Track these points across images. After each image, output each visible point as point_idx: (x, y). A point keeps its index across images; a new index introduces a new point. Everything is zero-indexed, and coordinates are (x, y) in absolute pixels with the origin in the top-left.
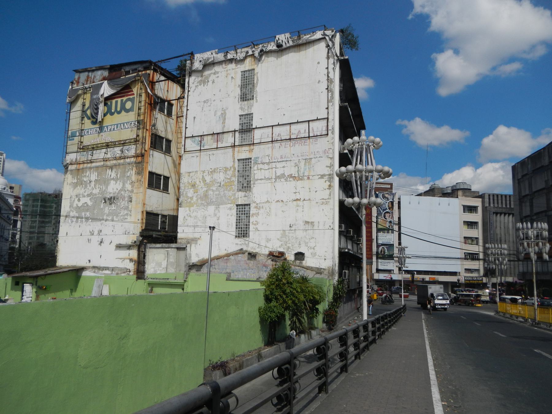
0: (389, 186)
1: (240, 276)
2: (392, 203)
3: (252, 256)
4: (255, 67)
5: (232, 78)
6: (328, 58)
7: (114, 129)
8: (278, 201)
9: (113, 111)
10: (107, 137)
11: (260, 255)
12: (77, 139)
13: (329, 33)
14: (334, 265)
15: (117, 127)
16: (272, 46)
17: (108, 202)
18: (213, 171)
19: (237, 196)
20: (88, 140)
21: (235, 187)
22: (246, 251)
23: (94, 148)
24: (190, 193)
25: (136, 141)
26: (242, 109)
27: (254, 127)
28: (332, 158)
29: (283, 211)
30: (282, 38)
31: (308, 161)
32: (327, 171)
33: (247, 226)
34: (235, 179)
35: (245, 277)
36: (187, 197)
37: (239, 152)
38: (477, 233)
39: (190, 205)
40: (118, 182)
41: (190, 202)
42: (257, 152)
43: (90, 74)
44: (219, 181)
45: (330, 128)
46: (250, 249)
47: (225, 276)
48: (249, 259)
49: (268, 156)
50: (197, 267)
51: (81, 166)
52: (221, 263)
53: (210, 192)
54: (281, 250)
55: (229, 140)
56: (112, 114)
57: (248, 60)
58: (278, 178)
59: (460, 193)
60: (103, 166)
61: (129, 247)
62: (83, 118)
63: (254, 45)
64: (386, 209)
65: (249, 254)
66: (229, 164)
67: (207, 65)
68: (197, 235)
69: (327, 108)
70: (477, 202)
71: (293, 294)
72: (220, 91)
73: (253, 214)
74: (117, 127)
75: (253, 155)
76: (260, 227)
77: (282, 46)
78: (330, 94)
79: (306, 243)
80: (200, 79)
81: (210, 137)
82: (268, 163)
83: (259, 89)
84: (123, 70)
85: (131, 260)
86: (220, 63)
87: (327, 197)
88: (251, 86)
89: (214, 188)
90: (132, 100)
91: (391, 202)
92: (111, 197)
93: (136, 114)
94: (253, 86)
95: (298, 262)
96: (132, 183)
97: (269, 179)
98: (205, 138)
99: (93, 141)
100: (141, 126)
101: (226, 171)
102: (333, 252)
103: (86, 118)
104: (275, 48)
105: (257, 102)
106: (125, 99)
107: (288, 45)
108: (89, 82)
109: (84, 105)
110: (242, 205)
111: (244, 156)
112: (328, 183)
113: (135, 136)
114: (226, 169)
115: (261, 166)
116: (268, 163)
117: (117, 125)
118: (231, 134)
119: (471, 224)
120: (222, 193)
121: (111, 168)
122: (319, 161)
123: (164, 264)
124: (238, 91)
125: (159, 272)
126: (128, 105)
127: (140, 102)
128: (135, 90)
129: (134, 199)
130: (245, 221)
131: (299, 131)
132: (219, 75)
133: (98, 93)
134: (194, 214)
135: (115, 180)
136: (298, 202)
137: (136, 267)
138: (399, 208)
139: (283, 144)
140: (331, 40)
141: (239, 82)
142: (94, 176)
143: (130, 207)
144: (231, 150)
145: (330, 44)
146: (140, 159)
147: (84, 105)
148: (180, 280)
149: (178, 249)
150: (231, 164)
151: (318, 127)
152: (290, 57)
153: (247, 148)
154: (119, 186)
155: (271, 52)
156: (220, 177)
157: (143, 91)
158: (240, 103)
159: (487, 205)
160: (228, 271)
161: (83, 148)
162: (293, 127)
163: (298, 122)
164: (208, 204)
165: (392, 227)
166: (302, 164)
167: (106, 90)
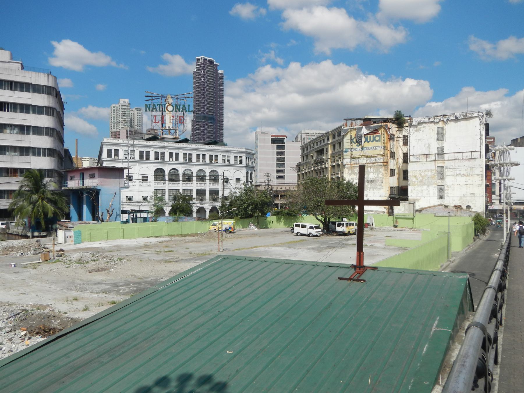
0: (492, 140)
1: (440, 215)
3: (446, 207)
4: (444, 126)
5: (433, 130)
6: (480, 125)
7: (370, 149)
8: (458, 185)
9: (369, 140)
10: (366, 152)
11: (450, 206)
12: (349, 153)
13: (480, 114)
14: (484, 211)
15: (372, 148)
17: (370, 182)
19: (437, 182)
20: (355, 153)
21: (437, 178)
22: (443, 205)
24: (414, 180)
25: (383, 155)
26: (438, 144)
27: (445, 153)
28: (483, 168)
29: (460, 189)
30: (458, 114)
31: (471, 168)
32: (480, 173)
33: (443, 194)
34: (436, 175)
35: (443, 215)
36: (412, 181)
37: (438, 163)
39: (414, 185)
40: (375, 173)
41: (414, 184)
42: (446, 164)
43: (353, 121)
44: (428, 175)
45: (482, 155)
46: (445, 204)
47: (434, 215)
48: (444, 208)
49: (452, 165)
50: (420, 211)
51: (353, 165)
52: (431, 210)
53: (424, 180)
54: (460, 204)
56: (368, 142)
57: (441, 122)
62: (351, 143)
64: (490, 158)
65: (445, 206)
66: (433, 168)
67: (420, 123)
68: (418, 198)
69: (480, 147)
71: (482, 222)
72: (427, 135)
73: (446, 190)
74: (372, 148)
75: (445, 165)
76: (449, 195)
77: (458, 118)
78: (481, 141)
79: (471, 202)
80: (416, 129)
81: (422, 156)
82: (452, 169)
83: (447, 136)
84: (371, 121)
86: (426, 123)
87: (481, 184)
88: (442, 134)
89: (426, 178)
90: (379, 136)
91: (494, 152)
92: (371, 180)
93: (382, 143)
94: (444, 134)
95: (468, 209)
96: (383, 174)
97: (453, 175)
98: (420, 156)
99: (358, 154)
100: (385, 149)
101: (432, 171)
102: (483, 206)
103: (353, 143)
104: (454, 119)
105: (446, 141)
106: (375, 135)
107: (461, 118)
108: (353, 126)
109: (351, 137)
110: (440, 186)
111: (440, 165)
112: (481, 178)
114: (432, 171)
115: (449, 170)
116: (452, 169)
117: (372, 147)
118: (433, 155)
120: (430, 181)
121: (370, 167)
122: (477, 169)
123: (403, 210)
124: (436, 136)
125: (400, 213)
126: (377, 138)
127: (384, 137)
128: (380, 132)
129: (384, 182)
130: (442, 192)
131: (467, 156)
132: (426, 128)
134: (417, 189)
135: (373, 173)
136: (467, 185)
137: (388, 211)
139: (460, 161)
140: (481, 117)
141: (436, 132)
143: (382, 185)
144: (434, 162)
145: (481, 119)
146: (386, 164)
147: (351, 137)
148: (412, 216)
149: (410, 203)
150: (434, 168)
151: (476, 155)
153: (442, 162)
156: (429, 174)
157: (385, 133)
158: (437, 141)
160: (435, 212)
161: (352, 157)
162: (464, 154)
163: (466, 152)
164: (425, 184)
165: (494, 171)
166: (469, 170)
167: (364, 131)
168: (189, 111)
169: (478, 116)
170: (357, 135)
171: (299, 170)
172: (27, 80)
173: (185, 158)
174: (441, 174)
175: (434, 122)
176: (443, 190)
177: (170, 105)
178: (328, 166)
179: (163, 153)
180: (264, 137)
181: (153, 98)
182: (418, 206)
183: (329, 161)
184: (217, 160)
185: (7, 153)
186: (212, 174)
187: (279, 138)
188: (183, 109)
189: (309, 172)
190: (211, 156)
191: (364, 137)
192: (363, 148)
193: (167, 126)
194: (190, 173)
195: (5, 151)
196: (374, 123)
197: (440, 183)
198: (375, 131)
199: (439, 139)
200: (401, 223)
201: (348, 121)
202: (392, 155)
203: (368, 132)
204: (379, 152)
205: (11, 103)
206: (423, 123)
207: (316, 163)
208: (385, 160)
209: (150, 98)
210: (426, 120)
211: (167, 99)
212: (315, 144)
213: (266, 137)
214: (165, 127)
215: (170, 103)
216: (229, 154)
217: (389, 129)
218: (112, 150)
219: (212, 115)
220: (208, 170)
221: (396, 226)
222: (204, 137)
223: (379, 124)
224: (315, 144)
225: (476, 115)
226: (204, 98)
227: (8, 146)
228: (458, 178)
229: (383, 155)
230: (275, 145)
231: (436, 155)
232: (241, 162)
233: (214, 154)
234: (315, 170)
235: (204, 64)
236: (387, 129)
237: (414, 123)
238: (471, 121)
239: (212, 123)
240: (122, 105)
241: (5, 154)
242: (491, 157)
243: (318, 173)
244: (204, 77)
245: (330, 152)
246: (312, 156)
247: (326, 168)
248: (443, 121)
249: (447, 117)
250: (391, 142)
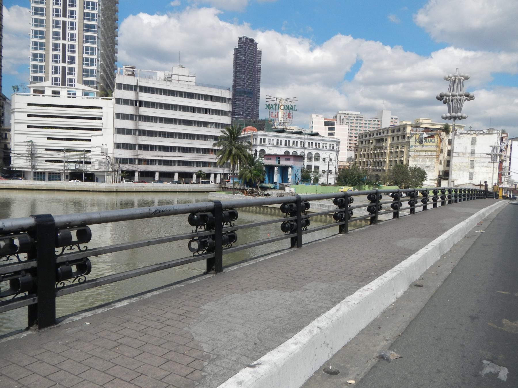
2: (507, 146)
10: (424, 149)
12: (413, 148)
13: (498, 132)
16: (482, 132)
18: (462, 163)
20: (417, 149)
21: (469, 167)
24: (455, 167)
25: (436, 151)
26: (472, 147)
30: (485, 131)
34: (469, 165)
39: (455, 171)
42: (475, 159)
56: (427, 142)
57: (474, 134)
58: (483, 166)
60: (424, 157)
61: (434, 180)
62: (415, 142)
64: (503, 149)
66: (467, 161)
67: (461, 134)
83: (477, 143)
85: (435, 183)
86: (465, 134)
90: (435, 139)
96: (435, 163)
106: (431, 138)
113: (436, 150)
114: (466, 163)
121: (427, 158)
124: (471, 142)
126: (433, 141)
127: (437, 140)
128: (435, 137)
133: (422, 136)
138: (511, 148)
141: (471, 140)
142: (421, 159)
146: (437, 157)
152: (487, 136)
154: (430, 163)
155: (481, 134)
156: (465, 164)
161: (416, 151)
164: (461, 171)
167: (425, 135)
168: (295, 110)
169: (497, 133)
170: (420, 137)
171: (357, 150)
172: (220, 95)
173: (301, 145)
174: (472, 165)
176: (473, 175)
177: (282, 105)
178: (387, 151)
179: (289, 141)
180: (318, 120)
181: (271, 100)
183: (388, 149)
184: (319, 146)
185: (208, 140)
186: (317, 155)
187: (331, 121)
188: (291, 108)
189: (368, 154)
190: (316, 143)
191: (425, 139)
192: (423, 146)
193: (280, 120)
194: (303, 154)
195: (207, 138)
196: (432, 131)
197: (471, 170)
198: (432, 136)
199: (472, 144)
201: (414, 128)
202: (442, 151)
203: (427, 136)
204: (434, 149)
205: (212, 109)
206: (463, 134)
207: (375, 148)
208: (438, 154)
209: (269, 100)
210: (465, 132)
211: (280, 101)
212: (375, 134)
213: (320, 120)
214: (279, 120)
215: (282, 104)
216: (326, 143)
217: (441, 135)
218: (262, 139)
219: (251, 90)
220: (314, 153)
222: (243, 110)
223: (435, 132)
224: (375, 134)
225: (496, 132)
226: (244, 74)
227: (208, 136)
228: (483, 168)
229: (436, 151)
230: (327, 127)
231: (470, 154)
232: (333, 148)
233: (318, 142)
234: (374, 153)
235: (245, 43)
236: (440, 135)
237: (457, 133)
238: (493, 135)
239: (250, 97)
240: (167, 77)
241: (207, 140)
242: (504, 148)
243: (377, 156)
244: (245, 55)
245: (389, 141)
246: (372, 143)
247: (385, 153)
249: (478, 131)
250: (441, 143)
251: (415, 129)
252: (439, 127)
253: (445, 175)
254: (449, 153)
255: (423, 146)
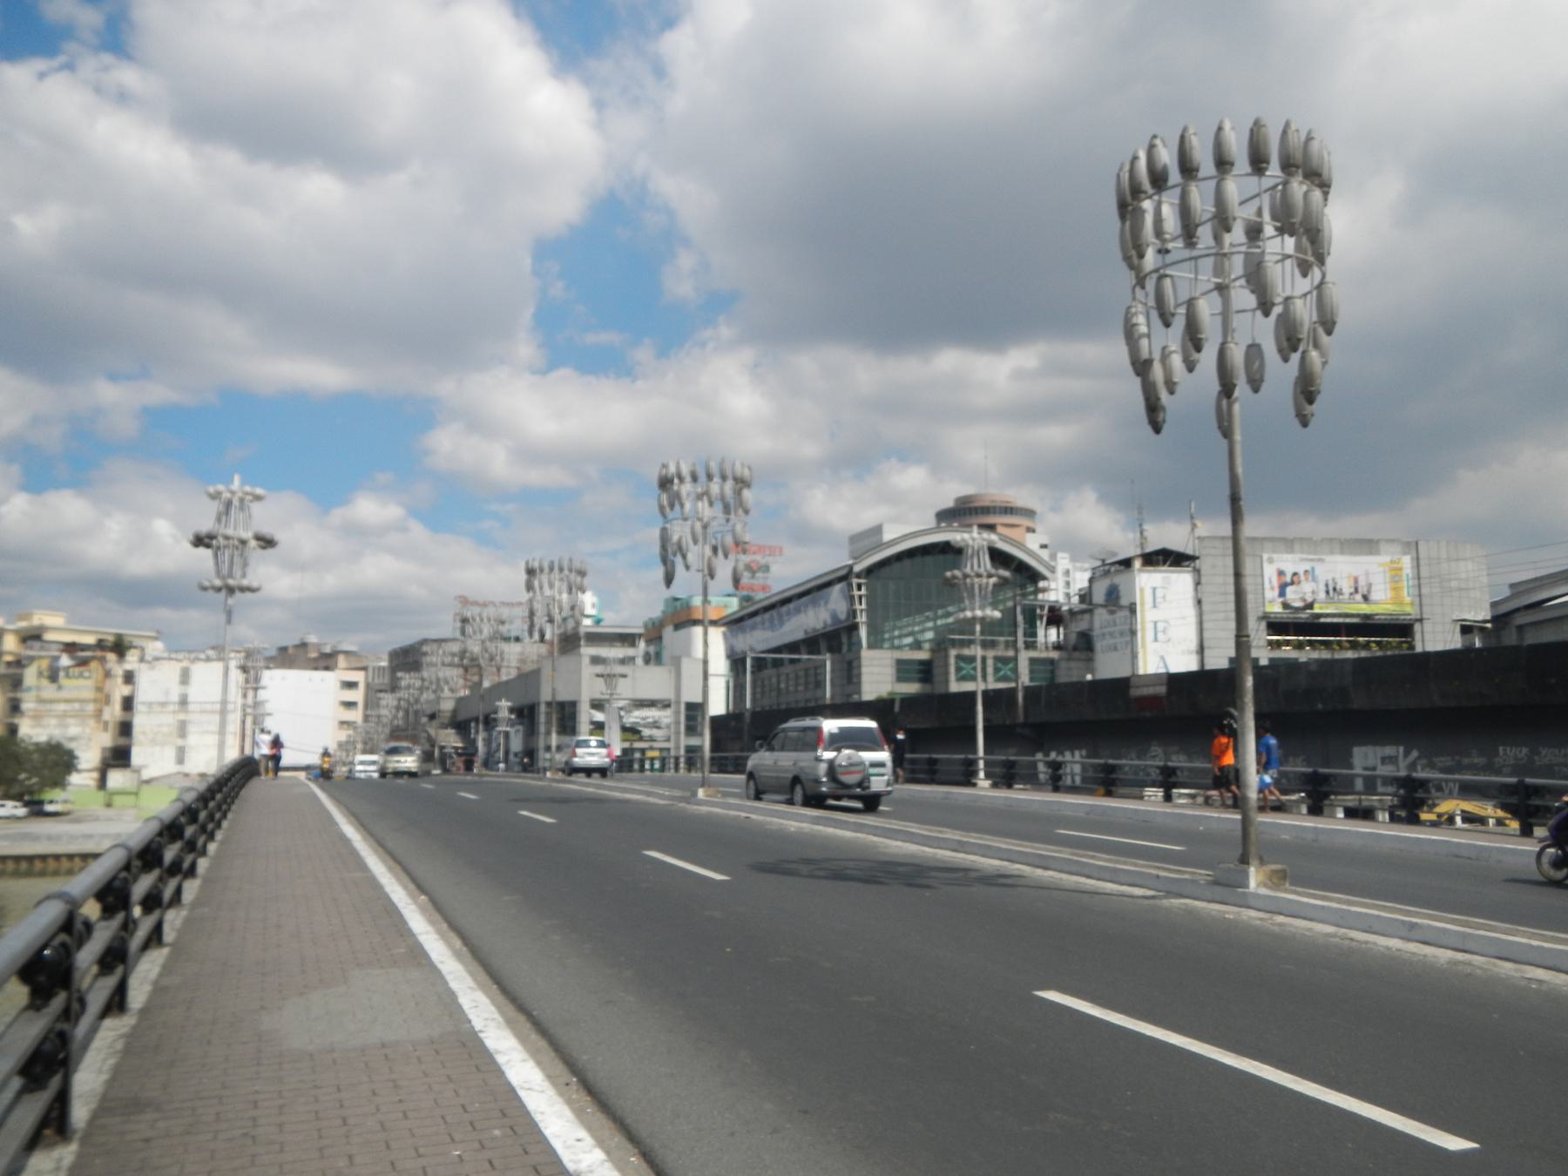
3: (186, 775)
10: (64, 694)
12: (33, 694)
16: (202, 656)
23: (52, 701)
25: (95, 701)
38: (356, 715)
50: (148, 782)
55: (171, 708)
59: (342, 661)
63: (190, 652)
67: (157, 659)
70: (359, 677)
85: (91, 779)
119: (350, 705)
142: (53, 721)
147: (39, 667)
148: (135, 790)
156: (165, 729)
159: (370, 680)
161: (41, 701)
167: (65, 661)
174: (182, 729)
175: (177, 660)
182: (146, 775)
192: (60, 688)
197: (180, 742)
198: (83, 663)
200: (118, 800)
202: (108, 700)
204: (89, 694)
210: (166, 655)
221: (109, 805)
229: (95, 701)
236: (103, 660)
237: (148, 657)
248: (189, 659)
251: (37, 644)
252: (90, 640)
253: (119, 757)
254: (128, 703)
255: (60, 688)
